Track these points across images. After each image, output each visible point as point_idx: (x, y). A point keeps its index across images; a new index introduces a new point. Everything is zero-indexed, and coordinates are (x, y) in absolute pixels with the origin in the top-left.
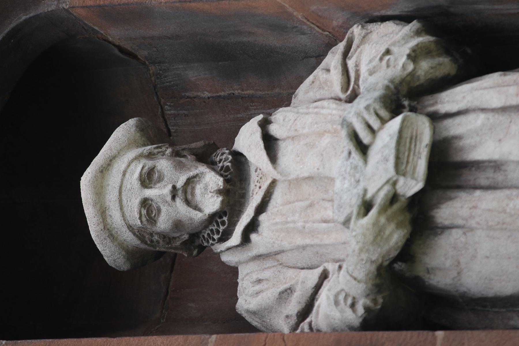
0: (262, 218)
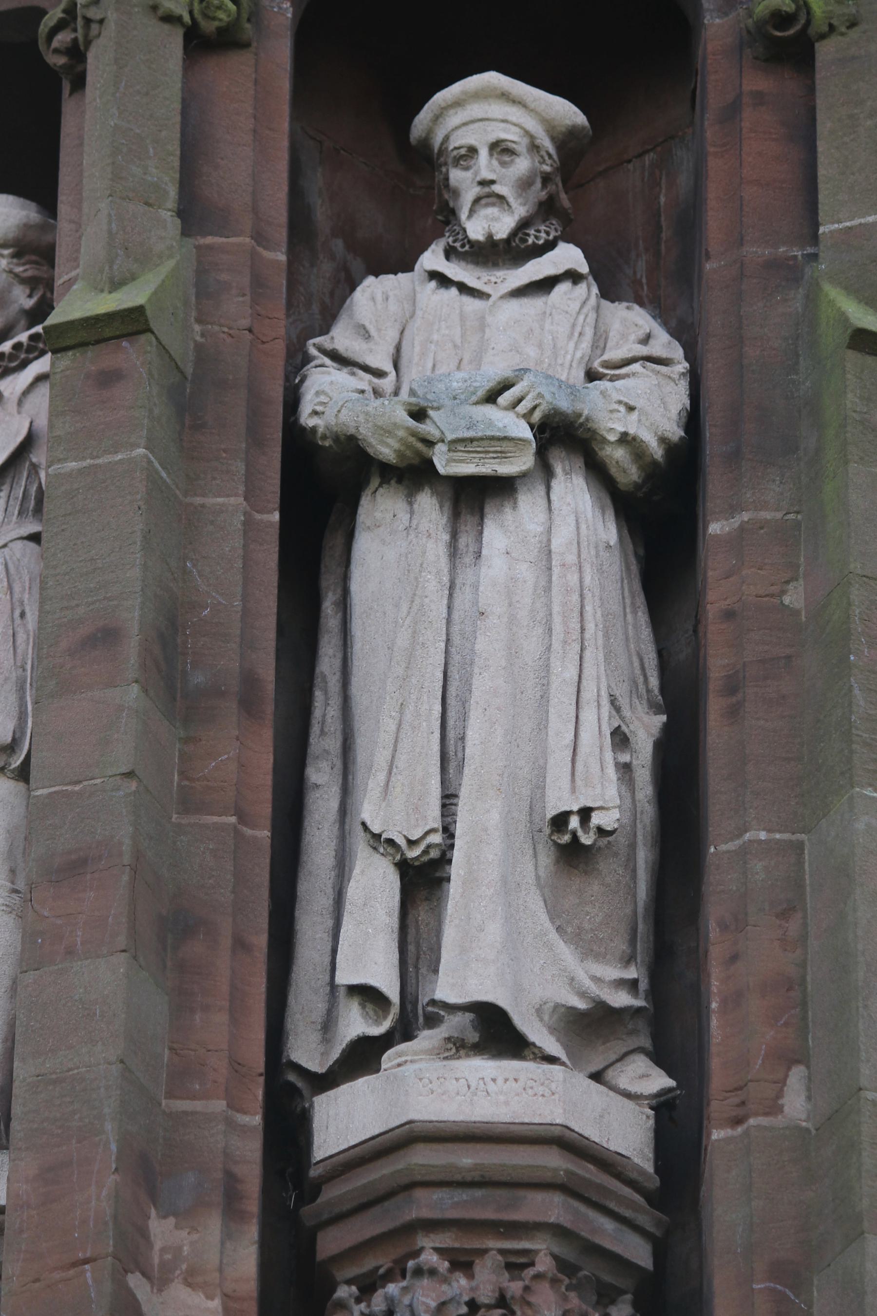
0: (454, 291)
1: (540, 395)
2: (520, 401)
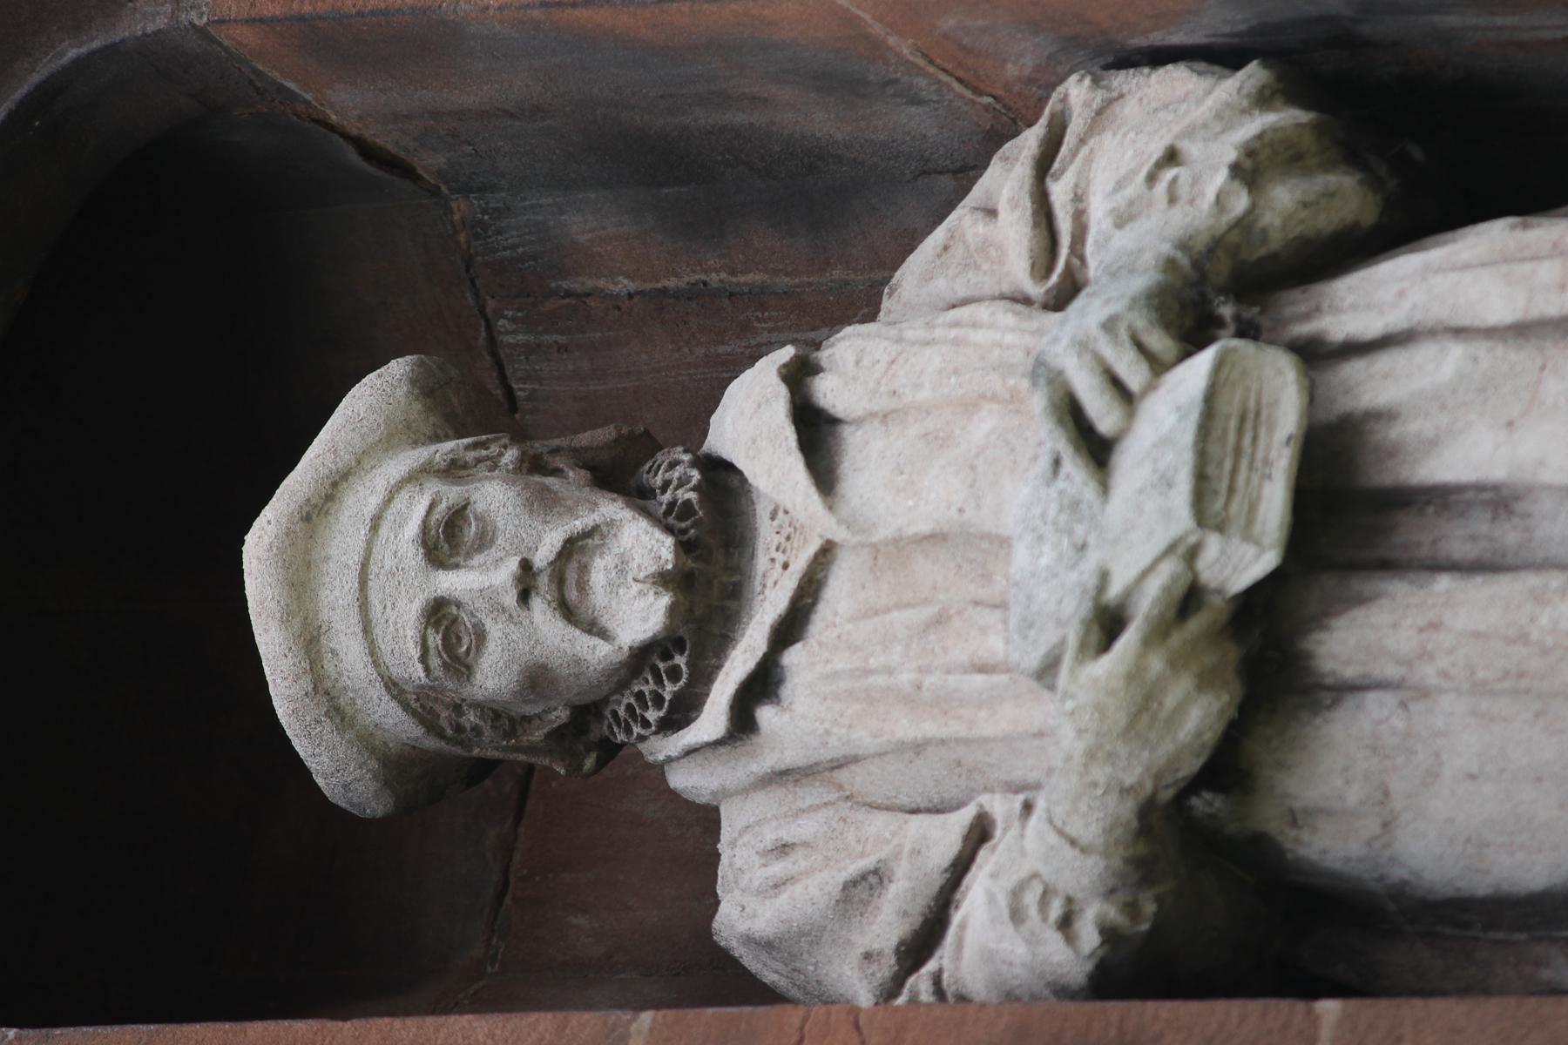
1: (1109, 326)
2: (1116, 384)
